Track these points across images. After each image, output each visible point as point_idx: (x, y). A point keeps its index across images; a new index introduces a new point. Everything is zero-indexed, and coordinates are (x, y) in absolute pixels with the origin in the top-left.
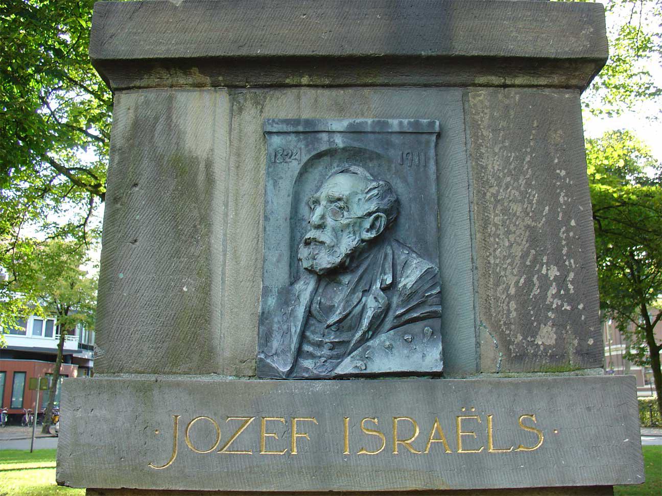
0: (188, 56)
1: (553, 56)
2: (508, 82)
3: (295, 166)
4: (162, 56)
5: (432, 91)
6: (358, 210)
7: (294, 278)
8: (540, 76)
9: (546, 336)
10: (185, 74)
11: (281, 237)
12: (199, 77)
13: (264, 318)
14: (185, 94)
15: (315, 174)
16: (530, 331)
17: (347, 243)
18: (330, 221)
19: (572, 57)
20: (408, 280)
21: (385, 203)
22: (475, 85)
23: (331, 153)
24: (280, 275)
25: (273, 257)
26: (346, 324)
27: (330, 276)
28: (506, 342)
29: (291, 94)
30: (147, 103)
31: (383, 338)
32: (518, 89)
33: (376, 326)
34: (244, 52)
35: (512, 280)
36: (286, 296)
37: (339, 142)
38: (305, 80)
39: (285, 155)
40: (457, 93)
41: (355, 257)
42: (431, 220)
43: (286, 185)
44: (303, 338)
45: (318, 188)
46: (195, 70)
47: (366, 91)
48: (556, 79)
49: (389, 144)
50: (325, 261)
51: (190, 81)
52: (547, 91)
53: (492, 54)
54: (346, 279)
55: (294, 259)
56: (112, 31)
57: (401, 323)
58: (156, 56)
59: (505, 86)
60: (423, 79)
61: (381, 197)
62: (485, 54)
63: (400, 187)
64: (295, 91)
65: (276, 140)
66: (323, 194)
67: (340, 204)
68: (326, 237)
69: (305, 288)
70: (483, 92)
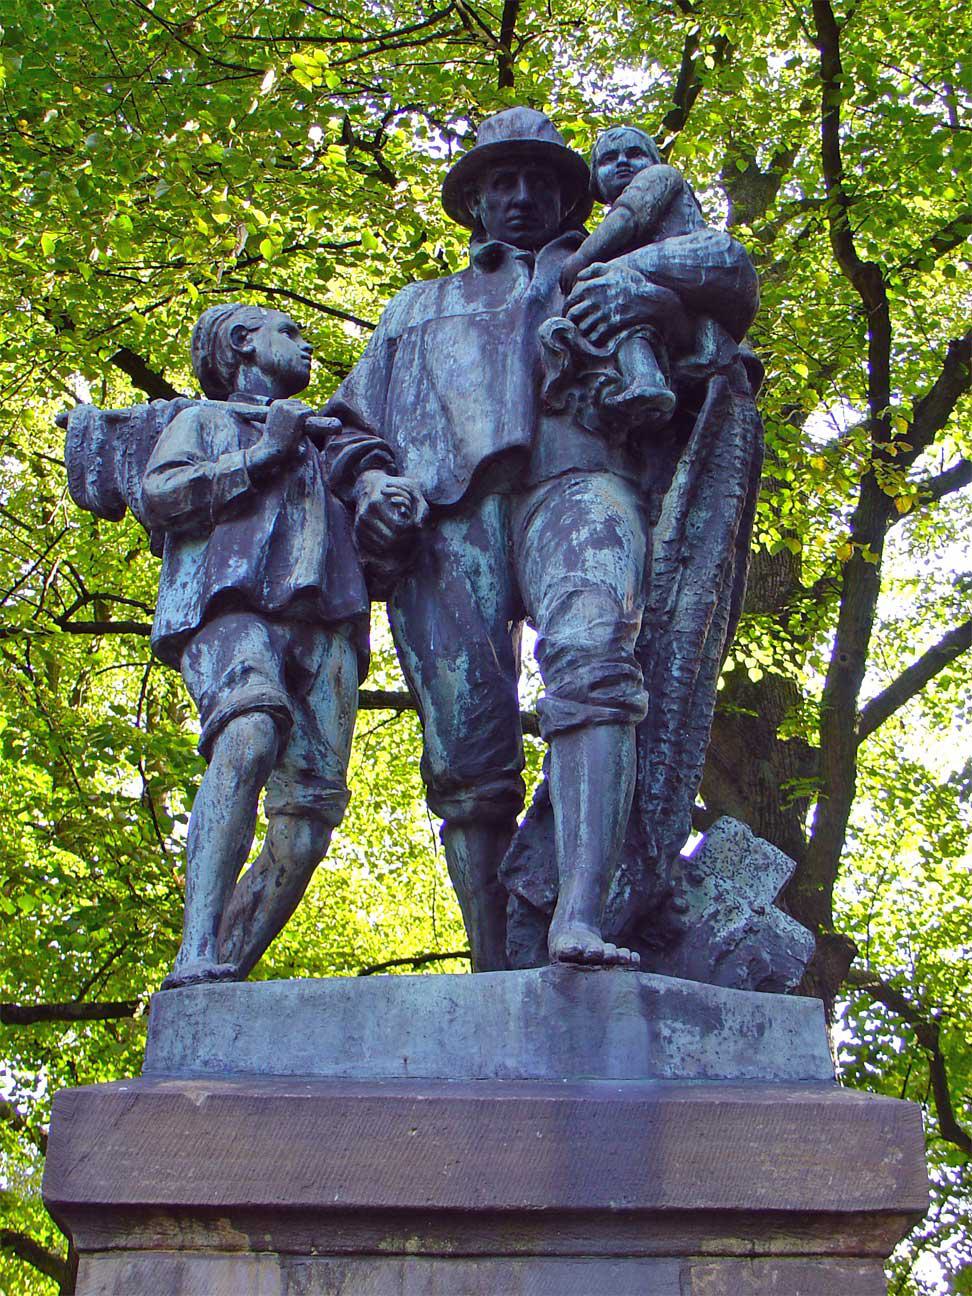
0: (216, 1202)
1: (833, 1208)
2: (759, 1249)
4: (170, 1201)
5: (629, 1265)
8: (815, 1237)
10: (207, 1227)
12: (228, 1233)
14: (204, 1263)
19: (867, 1208)
22: (701, 1254)
29: (387, 1267)
30: (137, 1277)
32: (780, 1261)
34: (311, 1198)
38: (412, 1245)
40: (672, 1267)
46: (224, 1222)
47: (516, 1265)
48: (842, 1242)
51: (215, 1240)
52: (827, 1263)
53: (728, 1206)
56: (84, 1148)
58: (160, 1200)
59: (753, 1255)
60: (614, 1244)
62: (718, 1205)
64: (395, 1263)
70: (716, 1265)
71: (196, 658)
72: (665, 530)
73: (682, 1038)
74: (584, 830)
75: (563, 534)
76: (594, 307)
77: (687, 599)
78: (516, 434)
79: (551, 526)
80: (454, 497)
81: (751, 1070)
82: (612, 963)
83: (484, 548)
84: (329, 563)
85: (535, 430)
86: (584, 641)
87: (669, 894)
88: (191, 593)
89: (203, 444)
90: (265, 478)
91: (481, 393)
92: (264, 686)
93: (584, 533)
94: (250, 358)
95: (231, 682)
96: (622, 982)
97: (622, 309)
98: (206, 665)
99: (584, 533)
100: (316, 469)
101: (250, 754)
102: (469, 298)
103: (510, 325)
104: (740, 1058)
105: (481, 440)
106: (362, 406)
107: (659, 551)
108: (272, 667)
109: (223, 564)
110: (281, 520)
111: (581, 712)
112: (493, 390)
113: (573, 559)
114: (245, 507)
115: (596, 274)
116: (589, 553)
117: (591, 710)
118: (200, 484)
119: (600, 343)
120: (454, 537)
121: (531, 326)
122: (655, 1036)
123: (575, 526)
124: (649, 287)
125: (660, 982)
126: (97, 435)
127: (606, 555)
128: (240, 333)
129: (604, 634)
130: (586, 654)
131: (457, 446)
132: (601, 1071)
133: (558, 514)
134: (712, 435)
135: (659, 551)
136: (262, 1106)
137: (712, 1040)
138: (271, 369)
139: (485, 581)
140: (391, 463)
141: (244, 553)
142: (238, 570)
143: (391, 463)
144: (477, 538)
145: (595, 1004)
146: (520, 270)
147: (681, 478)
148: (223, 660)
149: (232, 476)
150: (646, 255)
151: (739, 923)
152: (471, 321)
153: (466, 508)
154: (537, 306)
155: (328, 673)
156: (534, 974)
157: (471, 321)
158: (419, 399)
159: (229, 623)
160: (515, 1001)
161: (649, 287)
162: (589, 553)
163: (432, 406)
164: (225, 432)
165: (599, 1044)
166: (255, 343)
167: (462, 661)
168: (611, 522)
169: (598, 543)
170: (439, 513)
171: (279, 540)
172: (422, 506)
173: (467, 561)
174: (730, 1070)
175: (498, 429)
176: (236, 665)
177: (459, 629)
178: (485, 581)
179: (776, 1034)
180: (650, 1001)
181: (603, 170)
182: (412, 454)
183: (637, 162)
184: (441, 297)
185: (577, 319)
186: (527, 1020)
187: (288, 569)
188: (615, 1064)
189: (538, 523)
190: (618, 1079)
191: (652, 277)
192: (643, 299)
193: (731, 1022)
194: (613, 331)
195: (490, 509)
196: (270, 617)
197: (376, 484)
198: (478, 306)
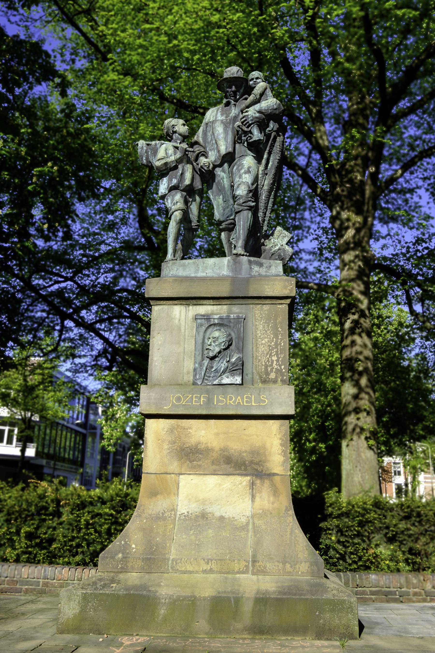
3: (204, 328)
6: (220, 341)
9: (273, 376)
11: (200, 347)
13: (195, 370)
16: (267, 374)
17: (217, 349)
18: (213, 344)
20: (233, 360)
21: (228, 339)
23: (214, 325)
24: (199, 358)
25: (197, 353)
26: (216, 371)
27: (212, 358)
28: (261, 377)
33: (224, 372)
37: (216, 321)
39: (201, 325)
42: (241, 343)
43: (201, 334)
45: (210, 334)
49: (230, 322)
50: (211, 354)
54: (217, 359)
60: (241, 302)
61: (227, 337)
63: (233, 335)
65: (199, 321)
67: (216, 339)
69: (206, 362)
71: (167, 199)
73: (256, 268)
74: (241, 231)
75: (239, 171)
76: (246, 120)
78: (231, 150)
80: (218, 163)
81: (268, 274)
82: (243, 255)
83: (225, 172)
86: (241, 194)
88: (166, 186)
89: (166, 154)
90: (179, 161)
91: (223, 140)
92: (181, 205)
93: (243, 171)
94: (175, 132)
95: (174, 205)
96: (245, 258)
97: (252, 120)
98: (169, 201)
99: (243, 171)
101: (178, 219)
102: (222, 115)
103: (230, 123)
104: (266, 272)
106: (201, 140)
107: (260, 172)
108: (182, 201)
109: (172, 180)
110: (183, 170)
111: (241, 208)
112: (226, 139)
113: (240, 177)
115: (247, 112)
116: (244, 175)
117: (243, 208)
118: (166, 164)
120: (218, 171)
121: (234, 124)
122: (251, 268)
123: (241, 169)
124: (257, 115)
125: (252, 259)
126: (145, 148)
127: (247, 175)
128: (173, 126)
129: (245, 192)
130: (242, 196)
131: (219, 151)
132: (241, 274)
133: (239, 166)
134: (272, 146)
135: (260, 172)
137: (261, 269)
138: (180, 134)
139: (225, 180)
140: (205, 155)
141: (176, 178)
142: (175, 181)
143: (205, 155)
144: (223, 171)
145: (240, 263)
146: (233, 108)
148: (173, 200)
150: (257, 107)
151: (277, 248)
152: (222, 122)
153: (221, 165)
154: (235, 118)
157: (222, 122)
159: (173, 192)
161: (257, 115)
162: (244, 175)
163: (214, 142)
164: (171, 151)
165: (241, 270)
166: (176, 128)
167: (221, 197)
168: (249, 168)
169: (245, 173)
170: (215, 167)
171: (182, 174)
172: (211, 166)
173: (221, 176)
174: (264, 274)
175: (226, 148)
176: (175, 201)
179: (273, 268)
182: (210, 153)
183: (258, 81)
184: (217, 114)
185: (242, 123)
186: (228, 266)
187: (185, 180)
189: (235, 168)
191: (259, 112)
192: (257, 118)
193: (265, 265)
194: (250, 125)
195: (226, 165)
197: (203, 160)
198: (223, 118)
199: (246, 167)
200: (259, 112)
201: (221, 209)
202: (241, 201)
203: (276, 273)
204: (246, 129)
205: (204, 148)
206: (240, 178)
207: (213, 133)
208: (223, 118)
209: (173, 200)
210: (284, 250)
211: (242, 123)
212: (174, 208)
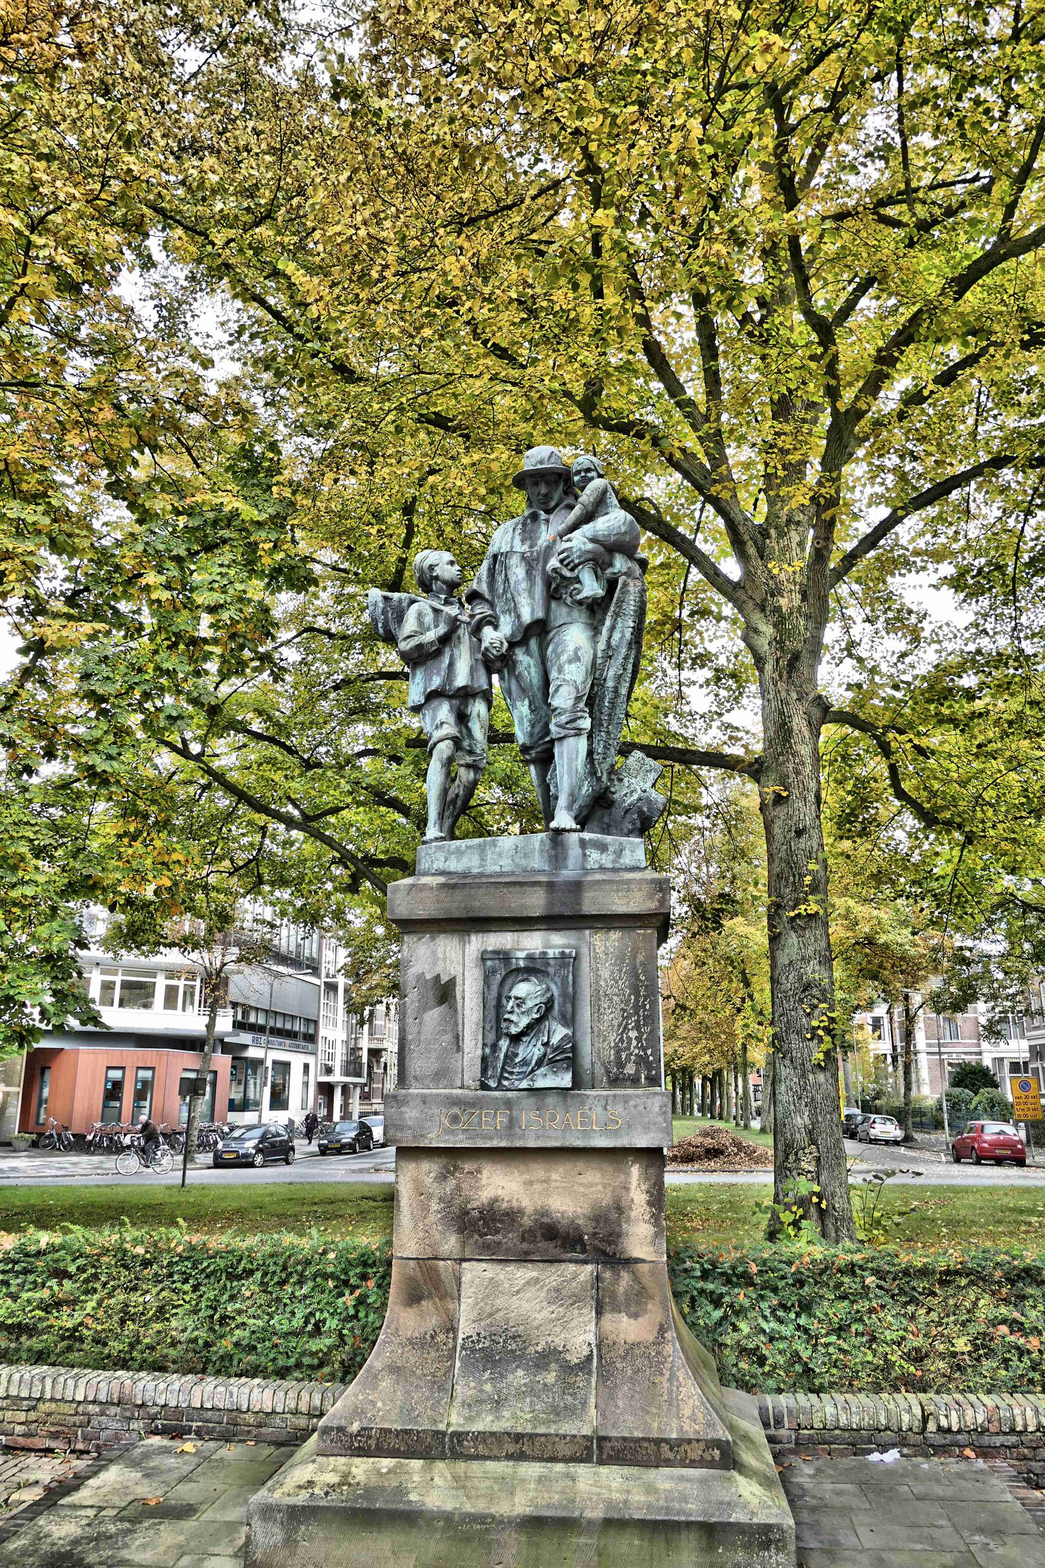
6: (530, 1004)
7: (498, 1038)
11: (492, 1014)
13: (484, 1059)
15: (509, 981)
16: (621, 1065)
17: (524, 1021)
20: (555, 1040)
24: (491, 1037)
28: (608, 1072)
31: (543, 1070)
35: (613, 1037)
36: (495, 1047)
37: (522, 964)
41: (530, 1027)
44: (503, 1069)
50: (514, 1030)
55: (498, 1029)
57: (552, 1061)
63: (554, 988)
66: (514, 993)
68: (514, 1017)
69: (504, 1044)
72: (602, 646)
77: (611, 673)
78: (540, 614)
79: (555, 650)
84: (472, 670)
85: (548, 610)
87: (607, 788)
88: (420, 688)
90: (445, 640)
94: (437, 578)
96: (574, 837)
98: (428, 719)
100: (464, 633)
105: (527, 618)
106: (484, 588)
108: (451, 719)
110: (452, 656)
111: (563, 732)
114: (438, 654)
118: (420, 646)
119: (572, 570)
120: (520, 655)
124: (590, 546)
127: (573, 667)
128: (431, 567)
129: (571, 702)
130: (565, 711)
134: (621, 601)
136: (454, 886)
138: (444, 582)
142: (436, 682)
144: (528, 653)
147: (608, 623)
148: (434, 718)
149: (432, 643)
150: (587, 529)
151: (635, 796)
155: (474, 714)
156: (542, 835)
158: (505, 591)
159: (435, 703)
160: (537, 845)
161: (590, 546)
166: (438, 571)
168: (577, 649)
169: (570, 662)
170: (512, 645)
171: (451, 665)
177: (523, 690)
178: (533, 670)
179: (627, 852)
180: (583, 843)
181: (576, 478)
188: (571, 866)
190: (568, 873)
191: (593, 540)
193: (611, 849)
194: (576, 566)
195: (533, 643)
196: (450, 697)
197: (488, 632)
199: (571, 648)
200: (593, 540)
201: (526, 724)
202: (563, 719)
203: (633, 863)
204: (568, 574)
205: (492, 605)
206: (560, 672)
207: (507, 579)
208: (525, 548)
209: (434, 718)
210: (649, 801)
211: (561, 561)
212: (437, 735)
